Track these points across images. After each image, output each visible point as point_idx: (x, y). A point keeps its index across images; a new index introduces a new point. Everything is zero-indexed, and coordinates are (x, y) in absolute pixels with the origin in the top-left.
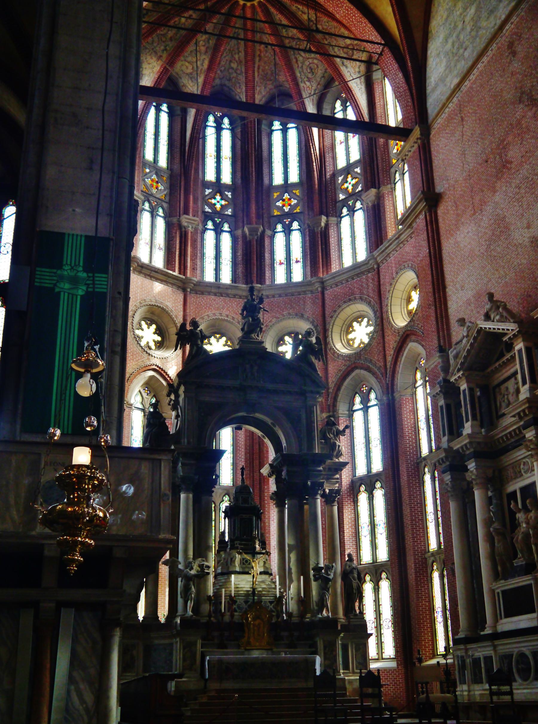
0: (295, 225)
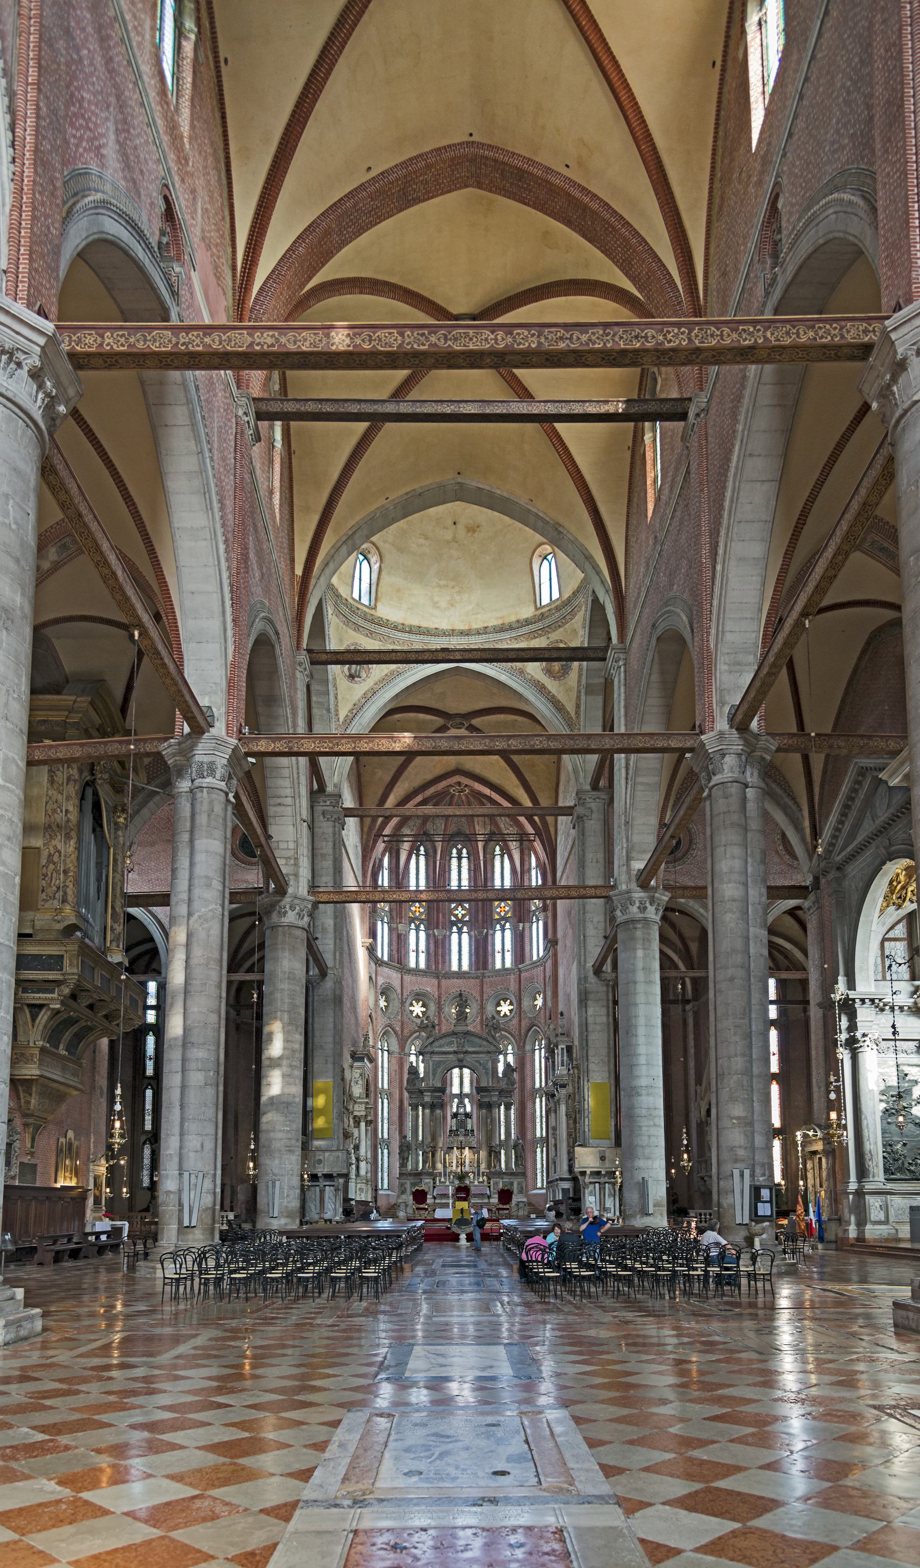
0: (508, 925)
